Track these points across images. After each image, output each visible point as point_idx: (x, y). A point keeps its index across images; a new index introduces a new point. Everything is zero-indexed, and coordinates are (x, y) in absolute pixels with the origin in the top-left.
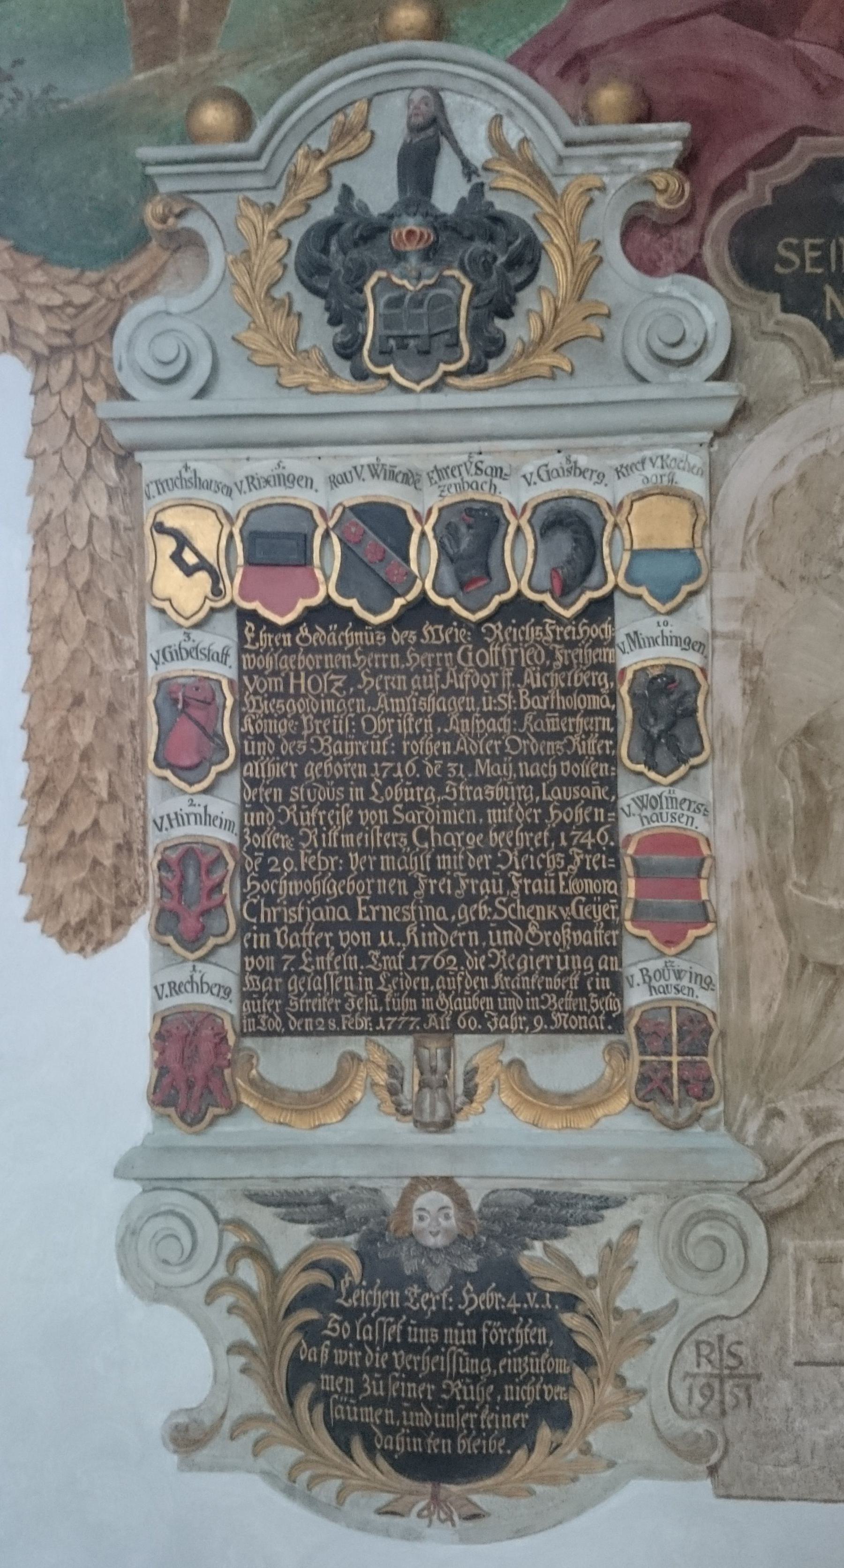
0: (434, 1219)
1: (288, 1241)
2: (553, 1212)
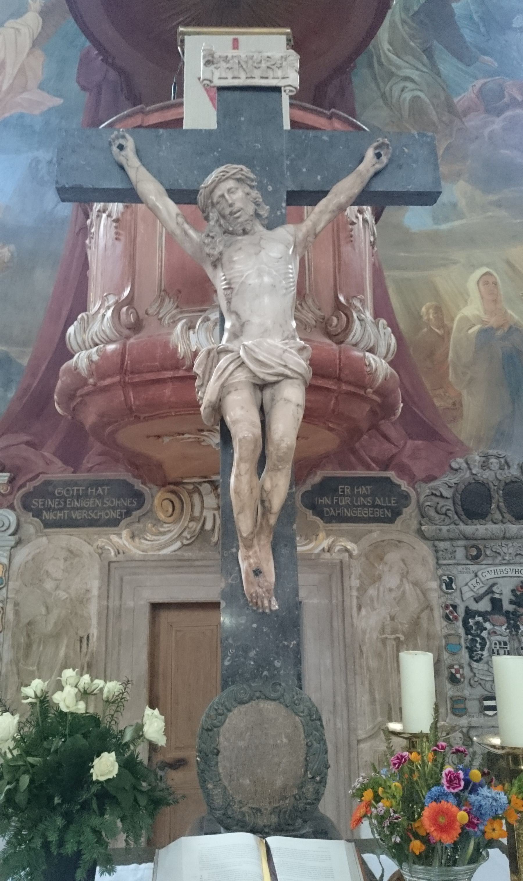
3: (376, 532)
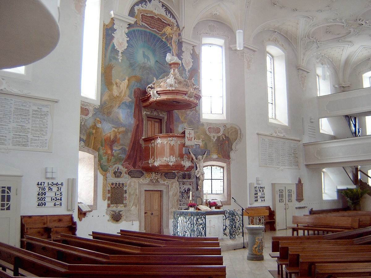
0: (117, 211)
1: (112, 212)
2: (121, 211)
3: (173, 180)
